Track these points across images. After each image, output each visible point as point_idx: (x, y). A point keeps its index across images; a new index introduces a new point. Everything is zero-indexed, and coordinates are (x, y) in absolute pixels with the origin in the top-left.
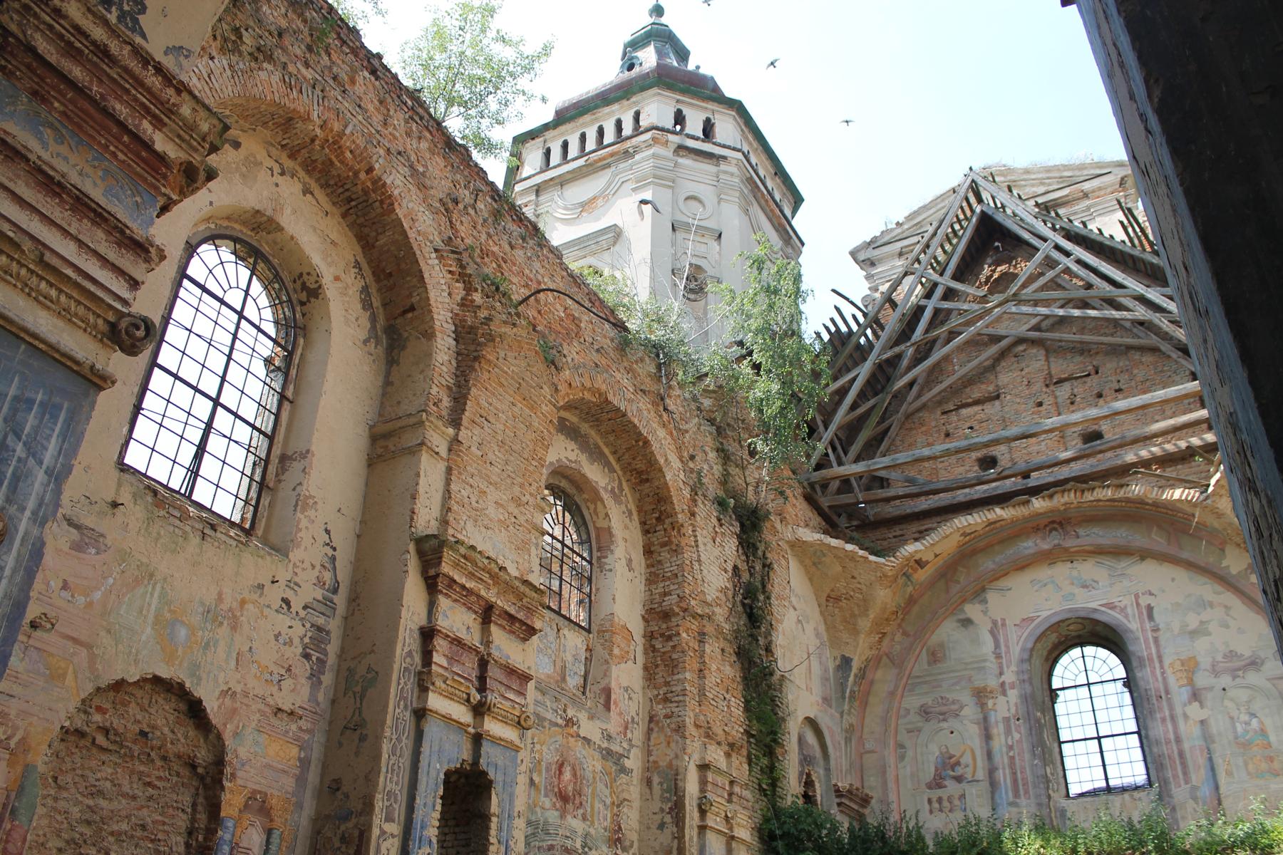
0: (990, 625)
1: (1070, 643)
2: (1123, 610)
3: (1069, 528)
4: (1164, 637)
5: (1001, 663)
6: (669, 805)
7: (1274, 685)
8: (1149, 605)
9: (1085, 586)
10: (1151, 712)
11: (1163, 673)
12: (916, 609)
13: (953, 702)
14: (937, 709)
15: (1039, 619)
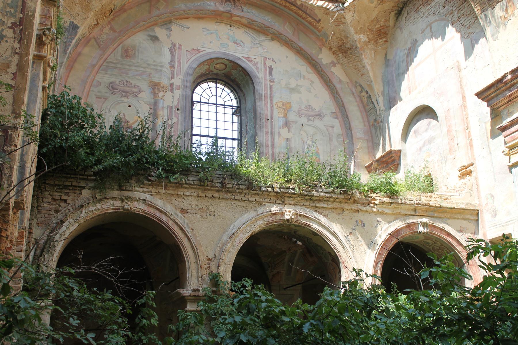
0: (170, 46)
1: (211, 77)
2: (256, 64)
3: (238, 4)
4: (275, 87)
5: (174, 71)
6: (13, 20)
7: (327, 129)
8: (271, 66)
9: (235, 43)
10: (262, 127)
11: (271, 107)
12: (124, 15)
13: (135, 87)
14: (122, 88)
15: (203, 53)
